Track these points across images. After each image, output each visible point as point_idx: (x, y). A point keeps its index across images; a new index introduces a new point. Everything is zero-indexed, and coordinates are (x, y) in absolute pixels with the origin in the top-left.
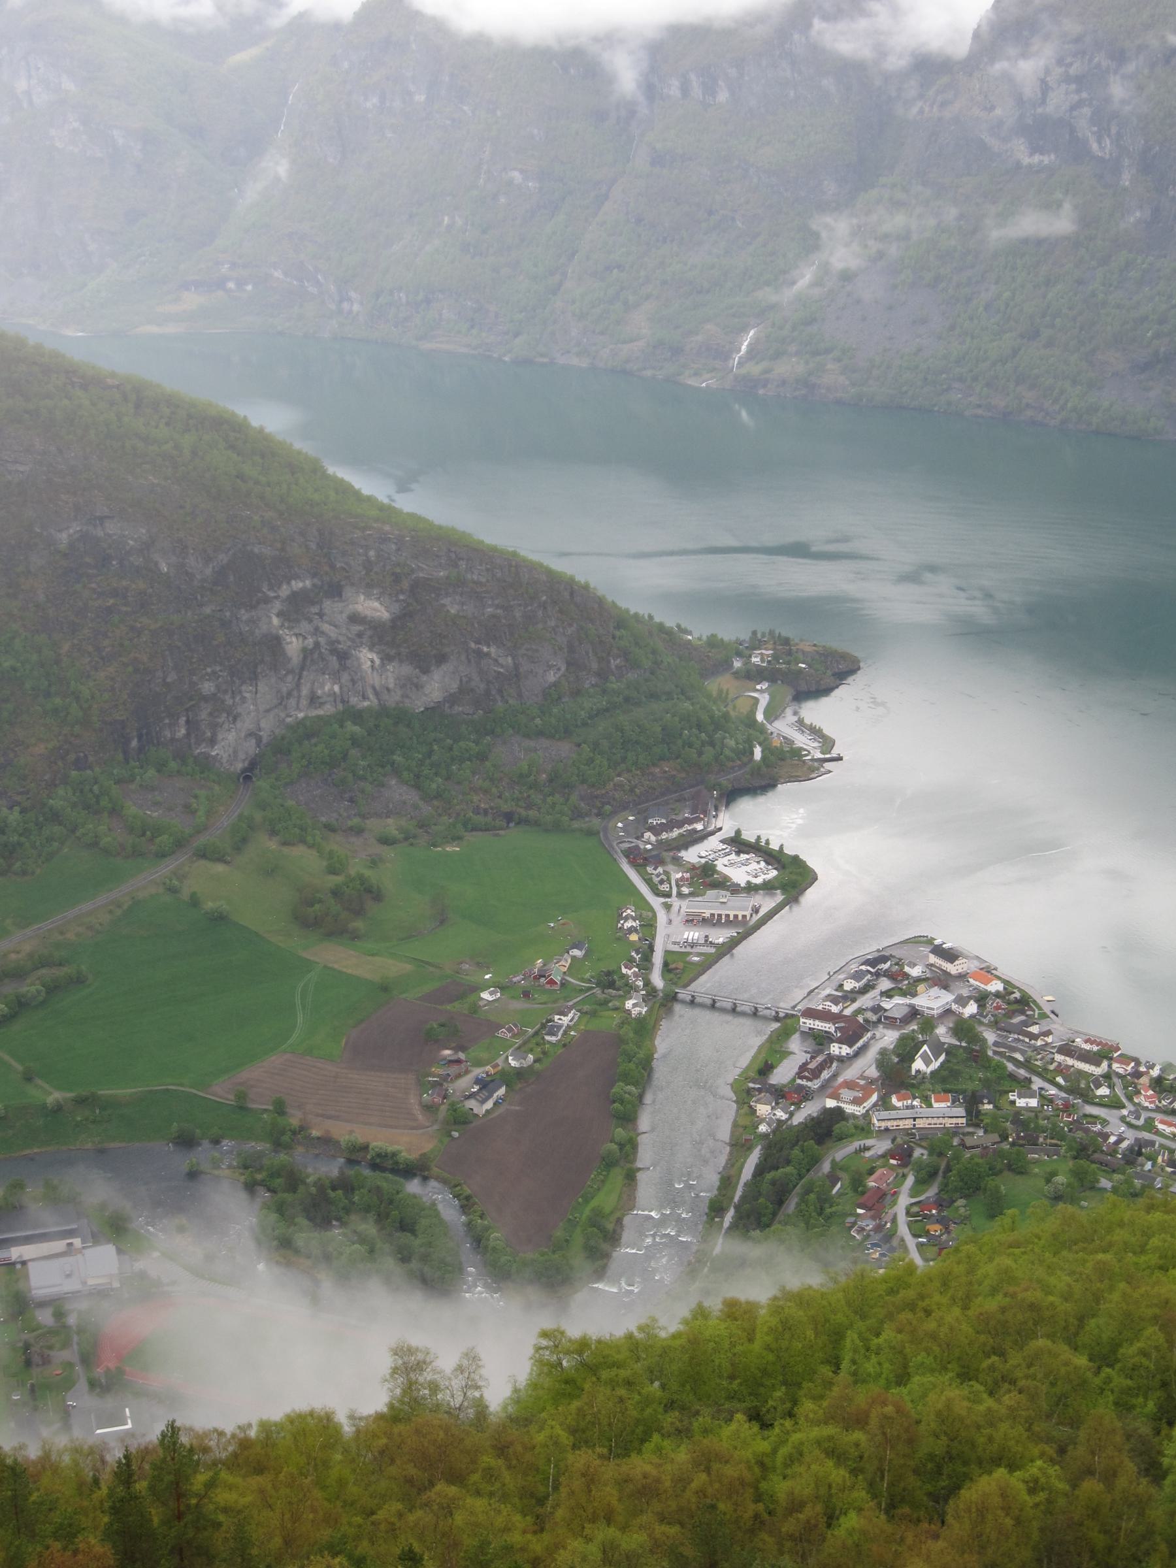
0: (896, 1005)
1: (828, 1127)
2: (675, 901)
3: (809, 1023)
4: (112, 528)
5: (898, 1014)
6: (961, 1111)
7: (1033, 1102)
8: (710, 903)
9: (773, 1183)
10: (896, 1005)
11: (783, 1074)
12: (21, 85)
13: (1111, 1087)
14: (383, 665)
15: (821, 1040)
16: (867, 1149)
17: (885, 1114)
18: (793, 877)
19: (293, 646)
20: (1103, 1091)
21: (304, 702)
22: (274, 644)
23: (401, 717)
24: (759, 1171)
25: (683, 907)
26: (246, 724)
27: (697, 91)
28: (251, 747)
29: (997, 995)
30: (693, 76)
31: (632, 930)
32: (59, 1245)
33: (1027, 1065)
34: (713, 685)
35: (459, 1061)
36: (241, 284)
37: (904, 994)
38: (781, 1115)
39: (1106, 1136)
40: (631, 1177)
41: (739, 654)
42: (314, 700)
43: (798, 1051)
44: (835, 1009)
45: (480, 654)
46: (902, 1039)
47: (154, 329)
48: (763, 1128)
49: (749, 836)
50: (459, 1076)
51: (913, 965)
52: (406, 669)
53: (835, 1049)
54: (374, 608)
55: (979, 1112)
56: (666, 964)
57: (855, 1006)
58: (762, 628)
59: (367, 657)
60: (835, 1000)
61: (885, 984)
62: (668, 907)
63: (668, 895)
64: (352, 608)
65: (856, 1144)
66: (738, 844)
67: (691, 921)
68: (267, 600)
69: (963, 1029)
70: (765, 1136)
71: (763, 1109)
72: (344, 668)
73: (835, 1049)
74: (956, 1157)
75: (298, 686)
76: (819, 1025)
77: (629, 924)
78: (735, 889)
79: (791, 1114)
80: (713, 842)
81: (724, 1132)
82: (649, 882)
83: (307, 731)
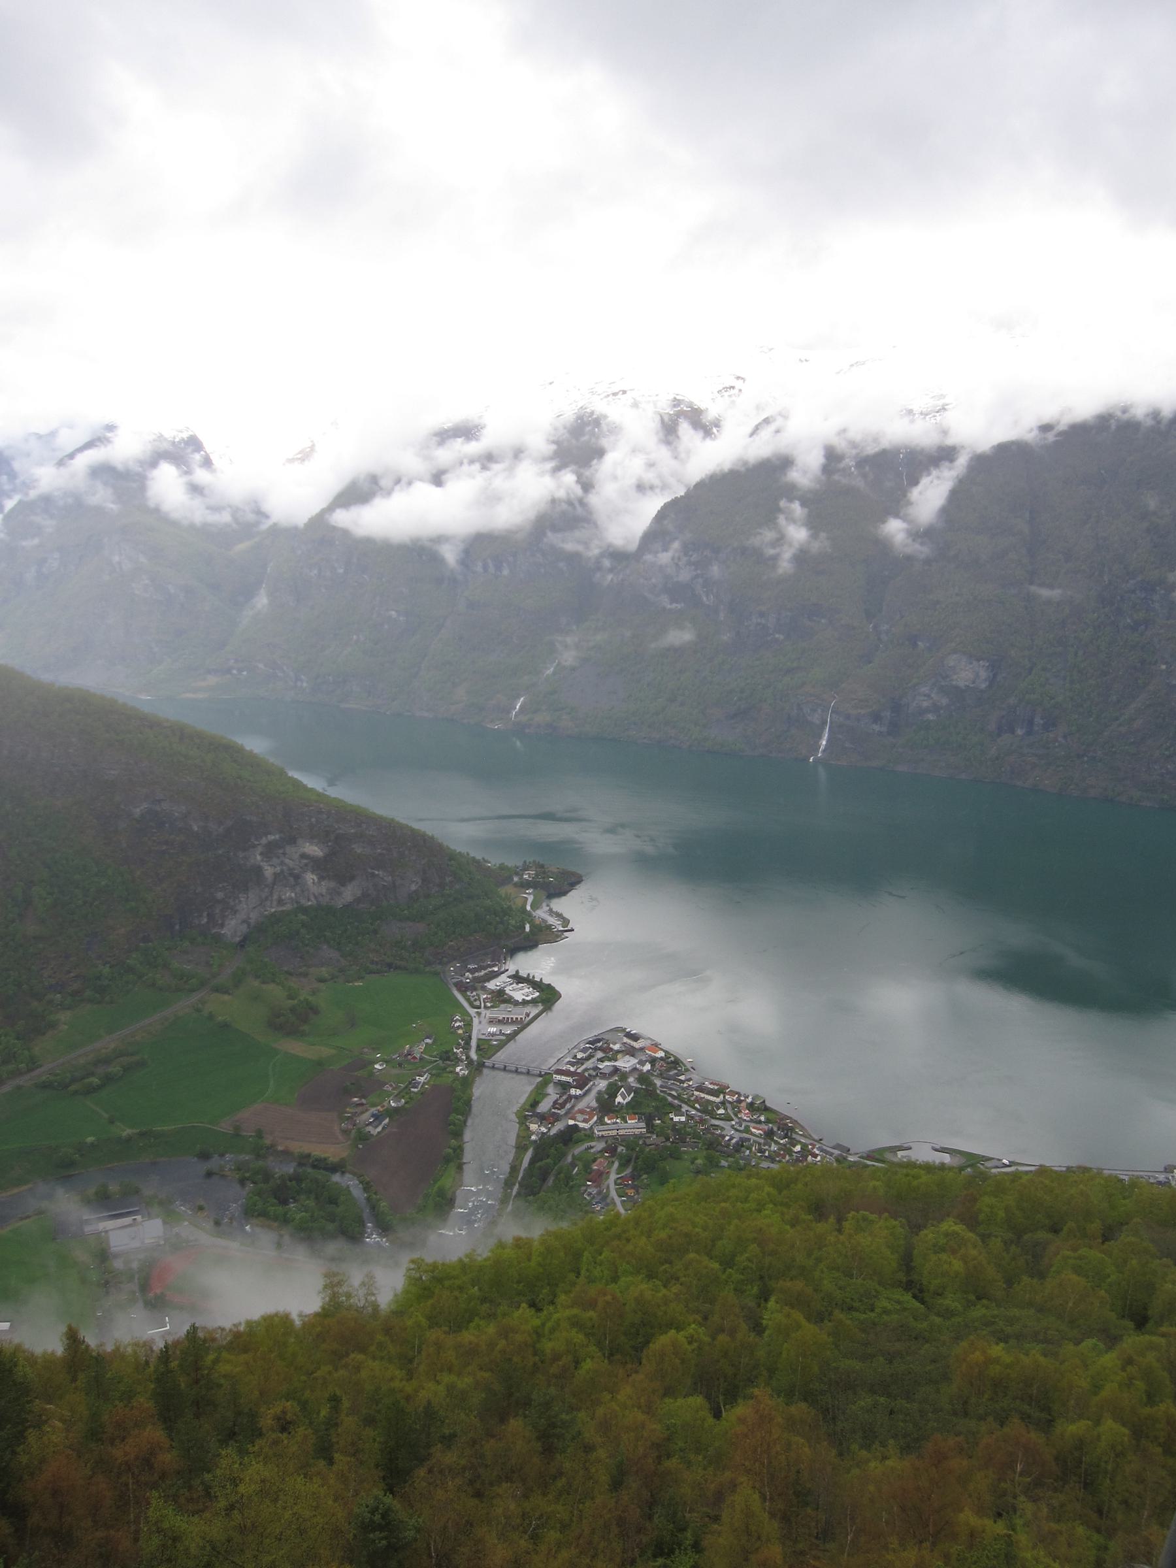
0: (605, 1066)
1: (570, 1136)
2: (482, 1010)
3: (558, 1077)
5: (607, 1071)
6: (643, 1125)
7: (683, 1119)
8: (501, 1012)
9: (540, 1168)
10: (605, 1066)
11: (544, 1106)
12: (116, 559)
13: (725, 1109)
14: (319, 882)
15: (565, 1086)
16: (592, 1147)
17: (601, 1127)
18: (548, 996)
19: (269, 871)
20: (721, 1111)
21: (275, 903)
22: (258, 870)
24: (532, 1162)
25: (488, 1014)
28: (244, 928)
29: (661, 1059)
30: (489, 561)
31: (459, 1027)
33: (678, 1097)
35: (362, 1104)
36: (240, 670)
37: (610, 1060)
38: (544, 1130)
39: (724, 1137)
40: (460, 1168)
41: (517, 874)
42: (280, 902)
44: (572, 1069)
45: (373, 875)
46: (610, 1085)
48: (533, 1137)
49: (523, 974)
50: (362, 1113)
51: (615, 1044)
52: (332, 884)
53: (573, 1091)
54: (314, 850)
55: (653, 1125)
56: (478, 1046)
57: (583, 1067)
58: (530, 859)
59: (310, 877)
60: (572, 1064)
61: (600, 1055)
62: (479, 1014)
63: (479, 1007)
65: (586, 1145)
66: (518, 978)
67: (492, 1022)
68: (254, 846)
69: (643, 1078)
70: (535, 1141)
71: (533, 1127)
73: (573, 1091)
74: (642, 1151)
75: (271, 894)
76: (564, 1078)
77: (457, 1024)
78: (516, 1003)
79: (549, 1129)
80: (503, 978)
81: (512, 1140)
82: (468, 1000)
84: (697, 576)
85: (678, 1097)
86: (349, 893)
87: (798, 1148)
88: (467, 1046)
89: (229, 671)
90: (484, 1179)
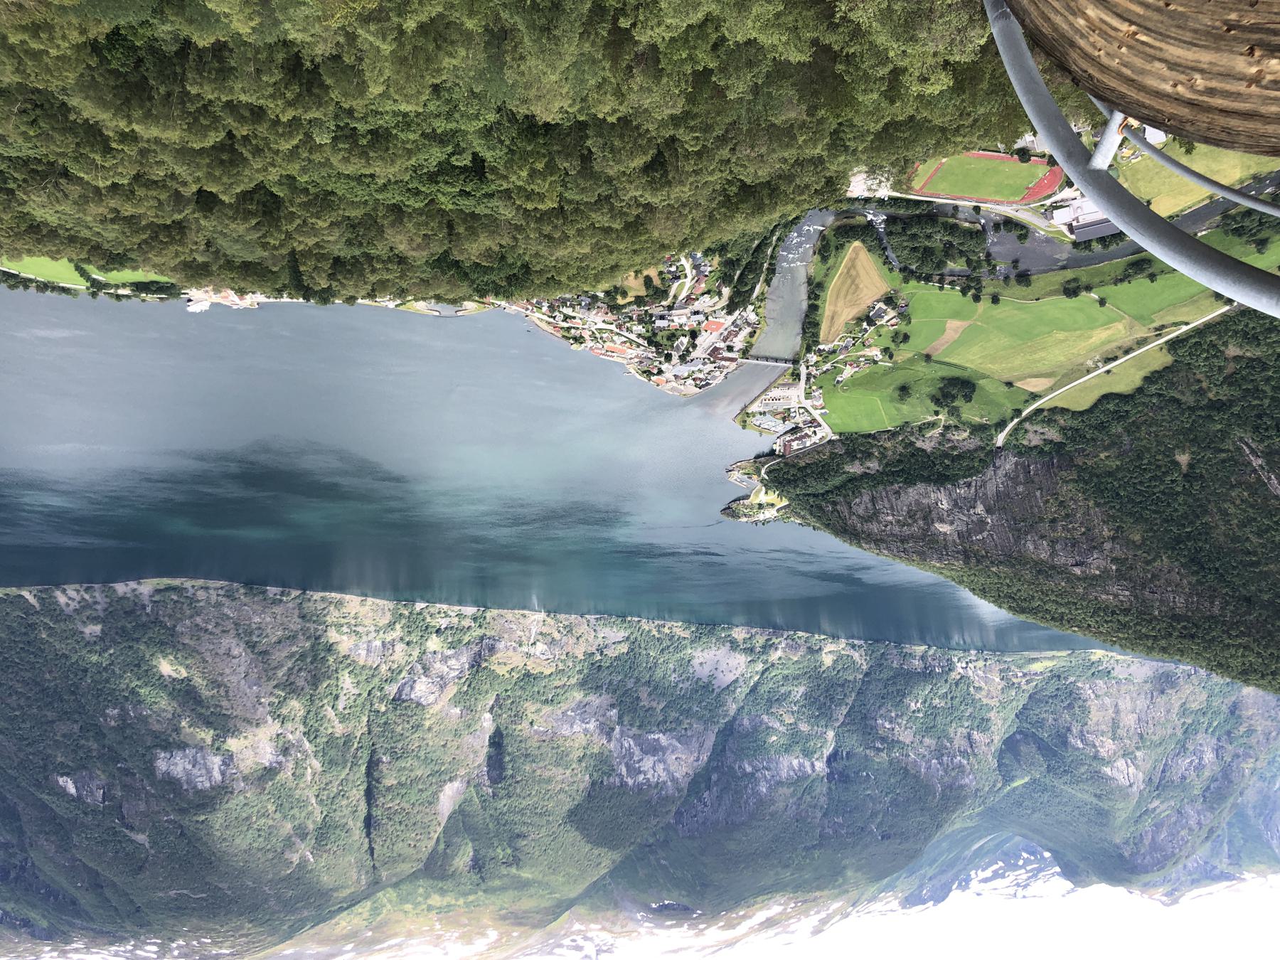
4: (1071, 561)
9: (746, 284)
15: (730, 349)
19: (980, 509)
22: (989, 511)
23: (927, 480)
26: (1001, 472)
27: (807, 764)
32: (1082, 222)
33: (639, 345)
34: (785, 502)
42: (969, 485)
43: (738, 342)
45: (892, 508)
47: (1059, 654)
53: (722, 345)
54: (944, 528)
60: (724, 367)
61: (701, 376)
64: (953, 527)
71: (752, 317)
72: (955, 501)
73: (722, 345)
83: (971, 471)
84: (639, 761)
85: (639, 345)
86: (914, 493)
87: (545, 309)
88: (809, 376)
89: (1025, 675)
90: (791, 270)
